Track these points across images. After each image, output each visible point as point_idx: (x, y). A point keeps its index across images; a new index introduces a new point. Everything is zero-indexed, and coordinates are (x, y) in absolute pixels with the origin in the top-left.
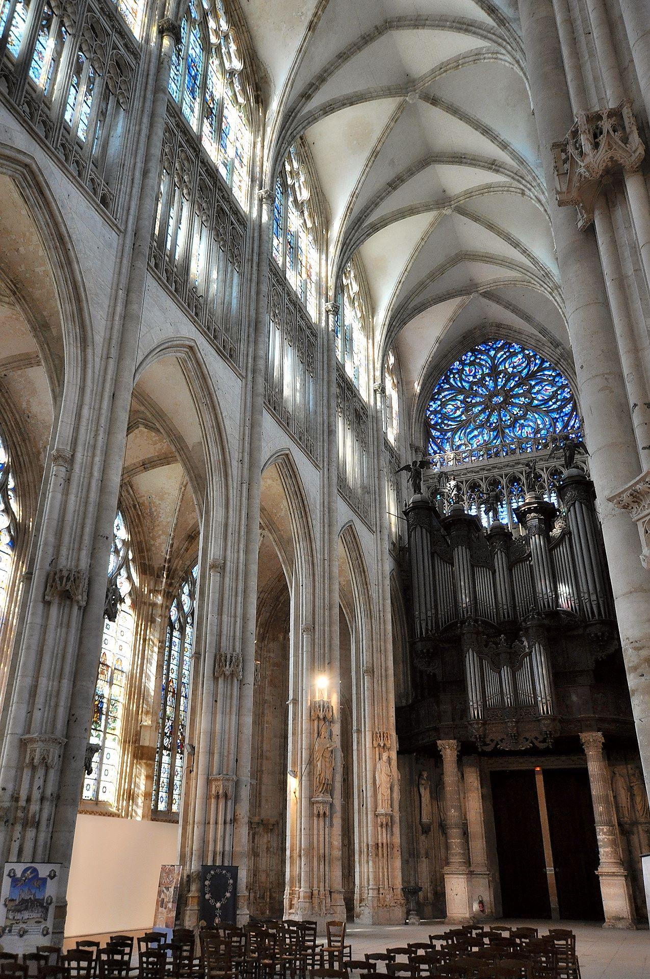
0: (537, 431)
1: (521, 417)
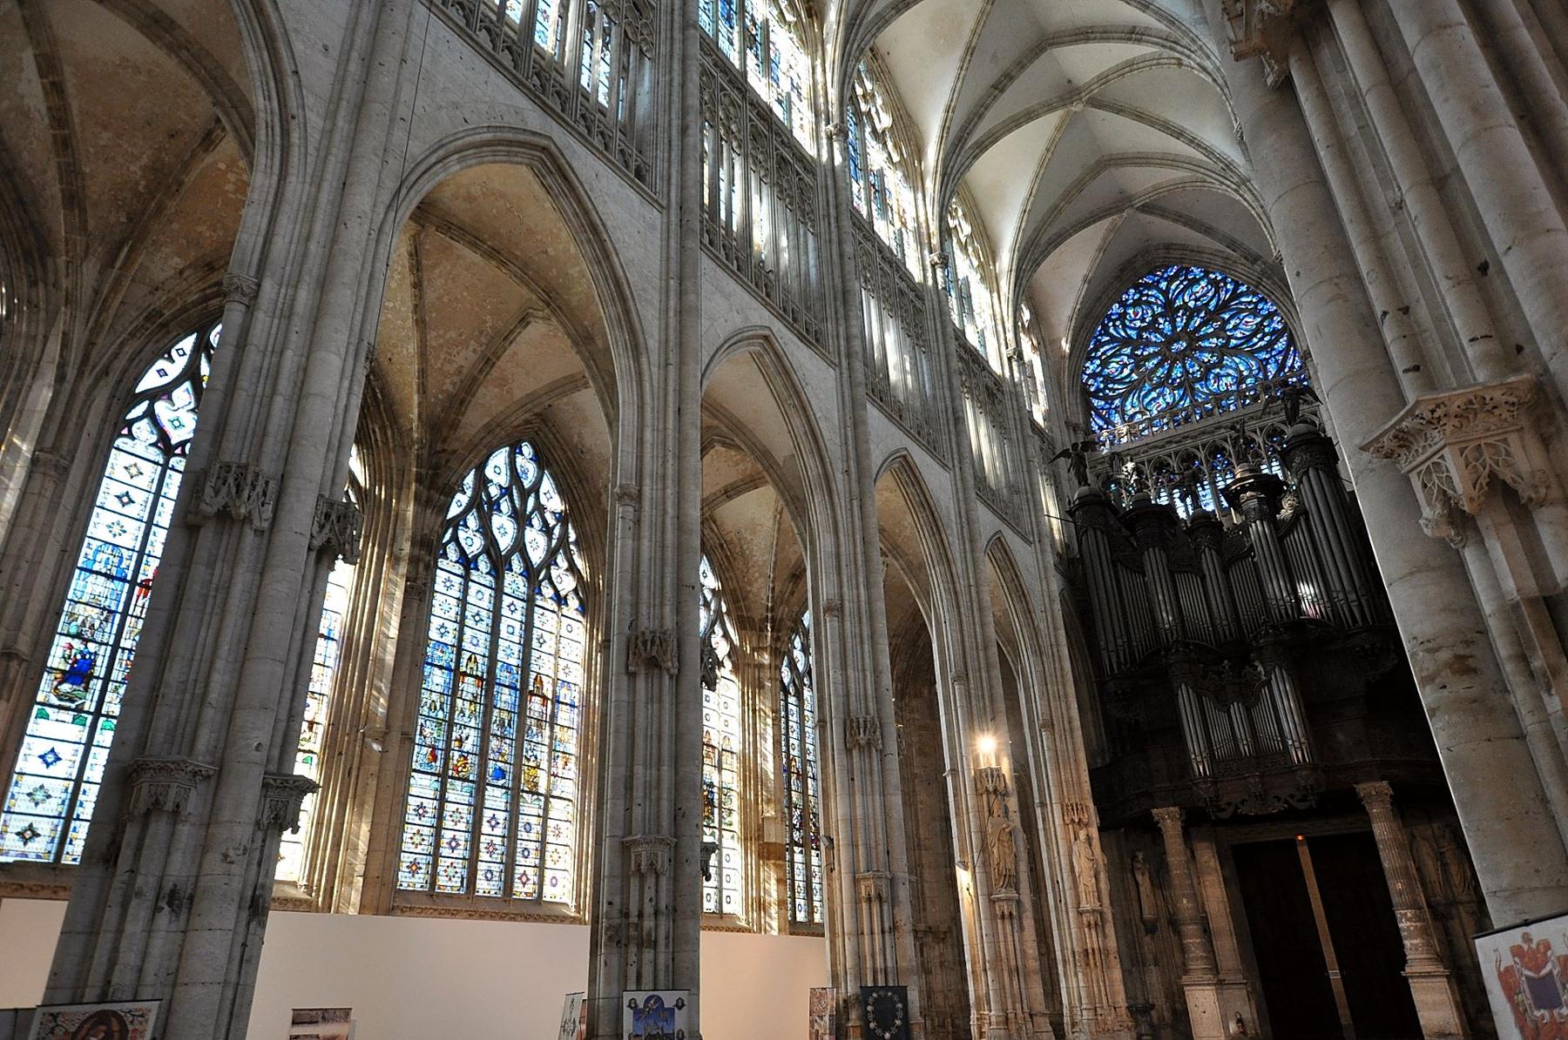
0: (1241, 380)
1: (1215, 366)
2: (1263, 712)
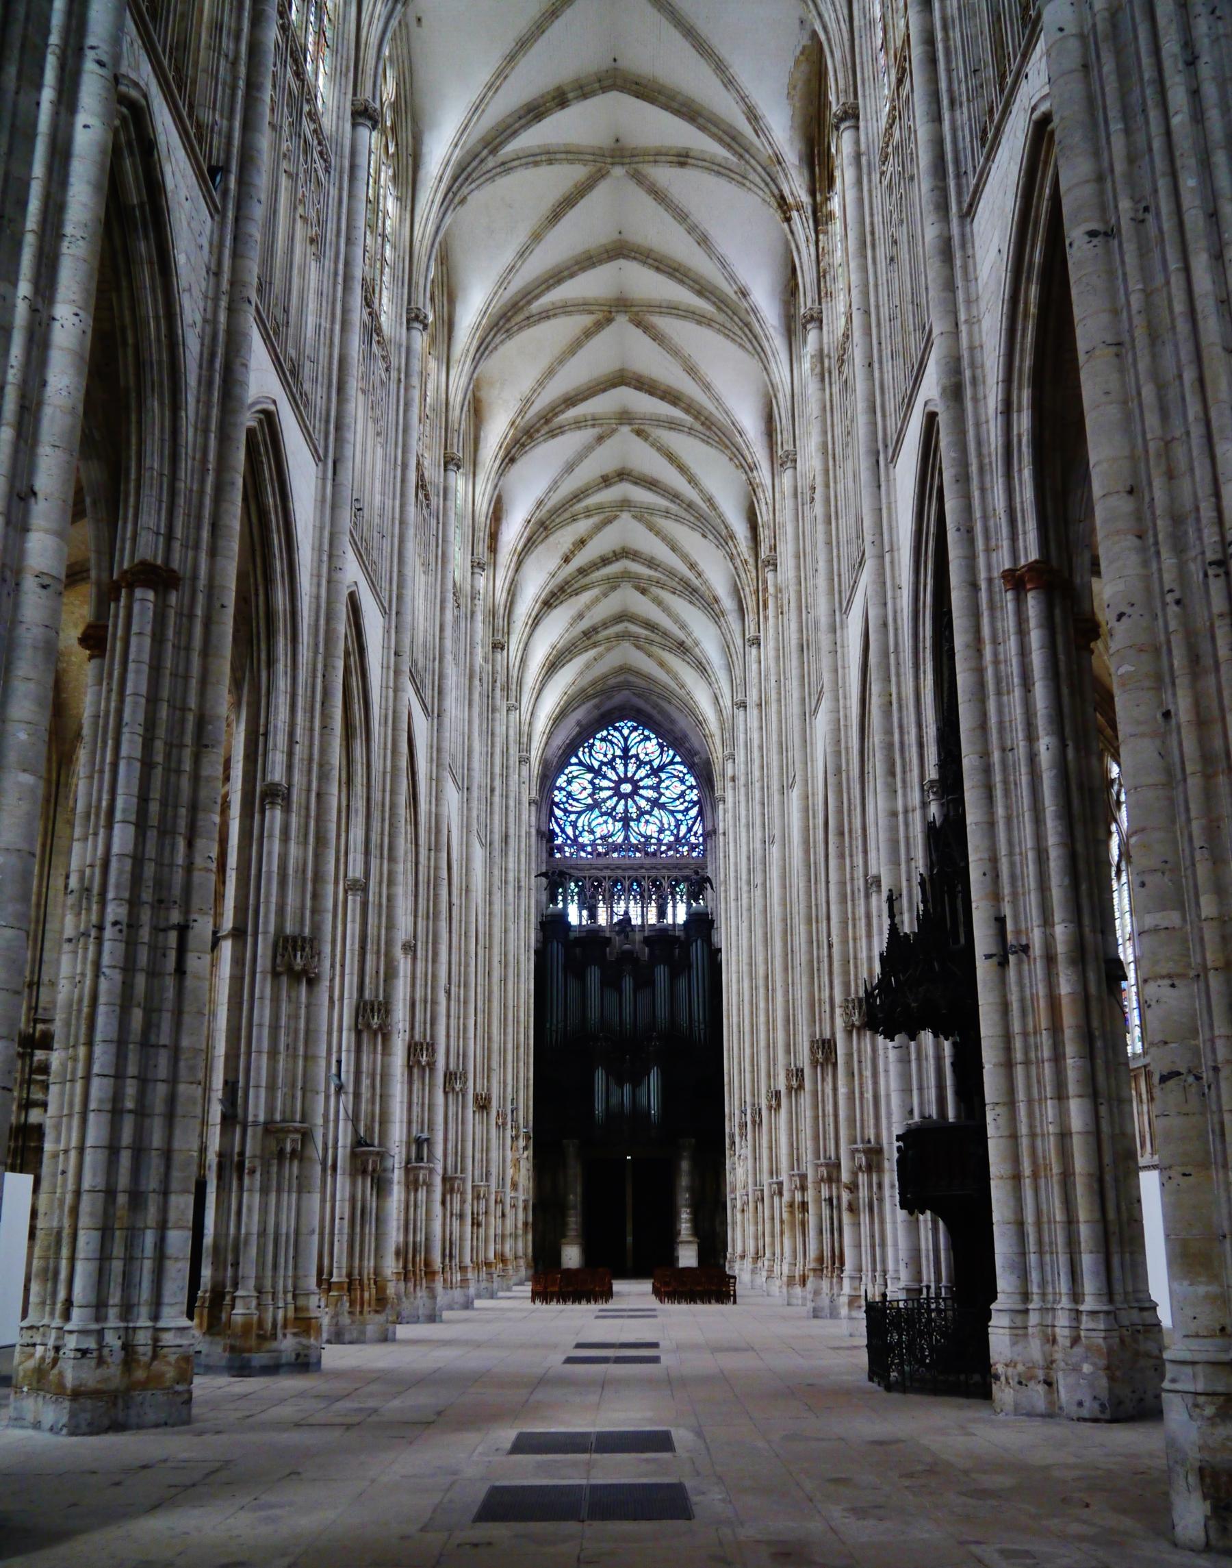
0: (661, 831)
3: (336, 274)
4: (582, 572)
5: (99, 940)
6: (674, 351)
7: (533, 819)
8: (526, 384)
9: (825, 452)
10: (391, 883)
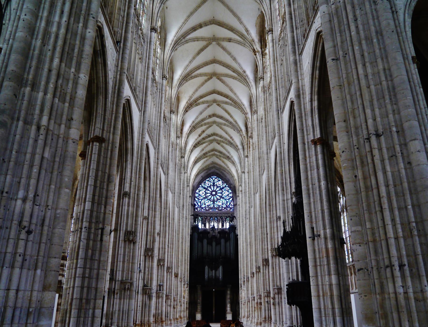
0: (223, 204)
2: (218, 272)
3: (145, 66)
4: (204, 139)
5: (81, 232)
6: (227, 85)
7: (190, 201)
8: (190, 93)
9: (265, 110)
10: (155, 217)
